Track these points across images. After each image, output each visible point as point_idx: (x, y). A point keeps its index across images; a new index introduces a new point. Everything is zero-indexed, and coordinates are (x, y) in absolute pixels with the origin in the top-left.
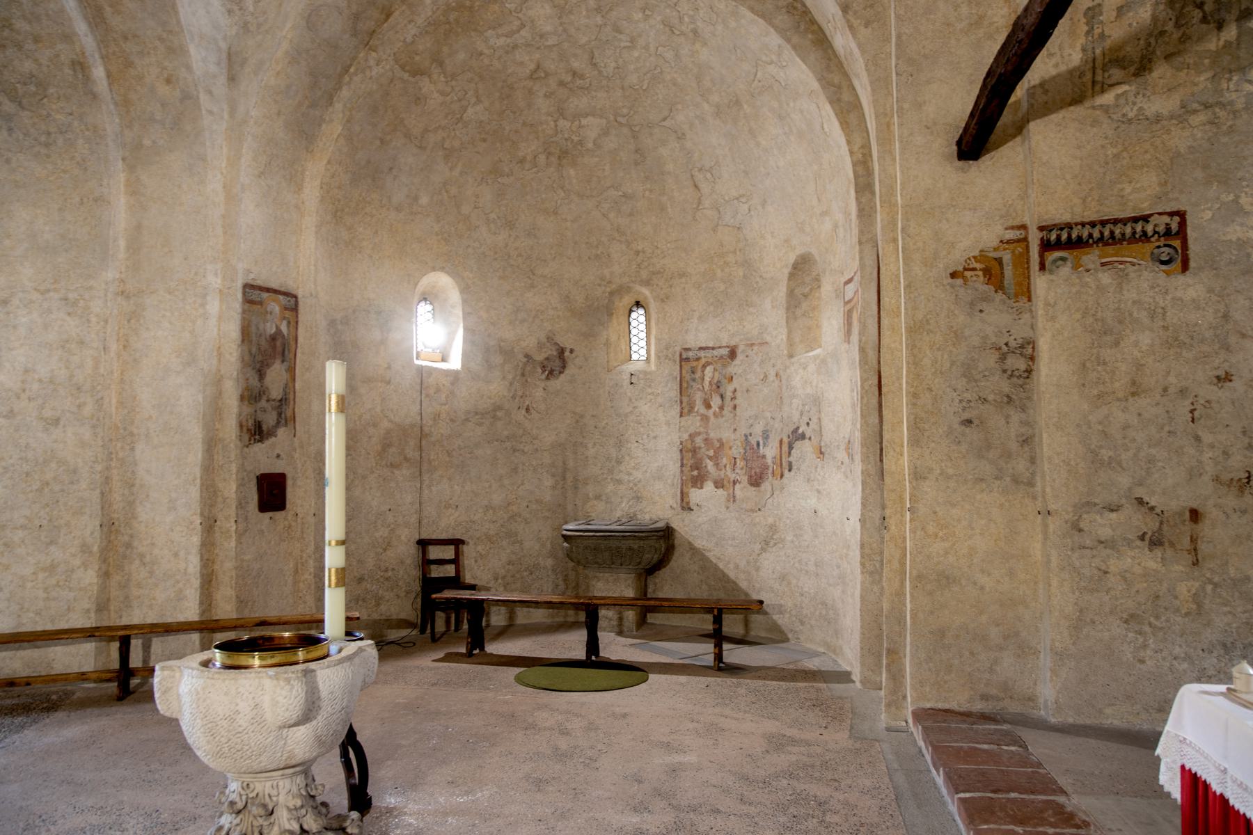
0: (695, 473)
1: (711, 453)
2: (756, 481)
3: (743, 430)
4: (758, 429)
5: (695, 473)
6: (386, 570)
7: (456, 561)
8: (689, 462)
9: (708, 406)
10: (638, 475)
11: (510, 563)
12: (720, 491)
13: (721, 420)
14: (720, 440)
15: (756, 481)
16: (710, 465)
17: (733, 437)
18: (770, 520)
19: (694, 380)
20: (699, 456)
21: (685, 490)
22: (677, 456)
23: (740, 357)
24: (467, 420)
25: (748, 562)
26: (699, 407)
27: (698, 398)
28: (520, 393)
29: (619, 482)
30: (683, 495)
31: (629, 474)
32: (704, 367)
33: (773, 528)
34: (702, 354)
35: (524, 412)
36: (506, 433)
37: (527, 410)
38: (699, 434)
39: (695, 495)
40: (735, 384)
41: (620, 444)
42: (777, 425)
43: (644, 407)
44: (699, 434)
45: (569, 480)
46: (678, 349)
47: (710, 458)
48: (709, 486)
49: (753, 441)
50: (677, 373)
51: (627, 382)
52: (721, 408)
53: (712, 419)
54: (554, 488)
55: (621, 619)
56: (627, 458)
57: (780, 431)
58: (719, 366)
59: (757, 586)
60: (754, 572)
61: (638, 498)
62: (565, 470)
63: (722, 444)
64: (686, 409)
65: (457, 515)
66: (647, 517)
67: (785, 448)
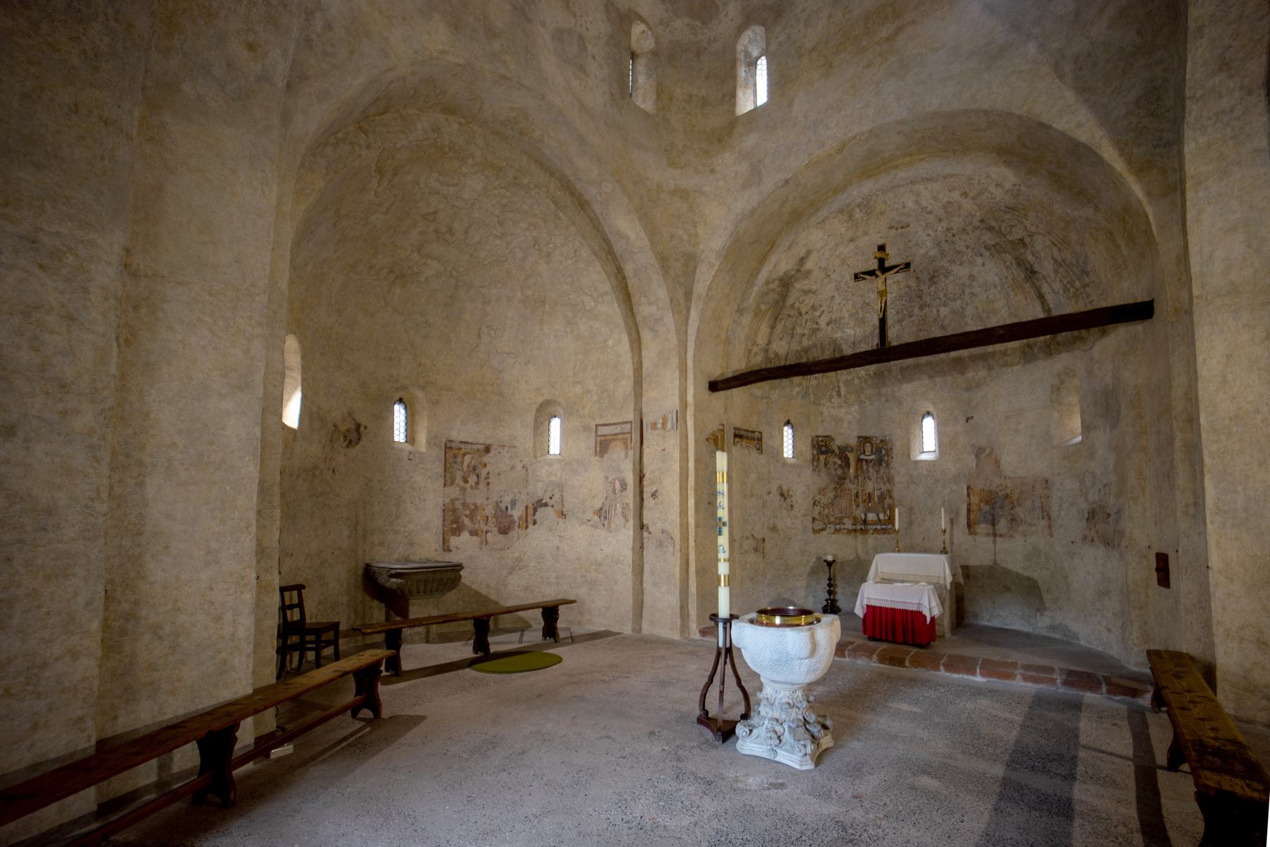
2: (504, 531)
3: (495, 498)
4: (507, 499)
9: (466, 481)
15: (504, 531)
16: (466, 521)
23: (493, 452)
26: (459, 481)
27: (459, 475)
32: (464, 455)
34: (463, 446)
46: (444, 440)
49: (503, 506)
50: (442, 456)
52: (477, 483)
57: (524, 500)
63: (476, 507)
67: (530, 511)
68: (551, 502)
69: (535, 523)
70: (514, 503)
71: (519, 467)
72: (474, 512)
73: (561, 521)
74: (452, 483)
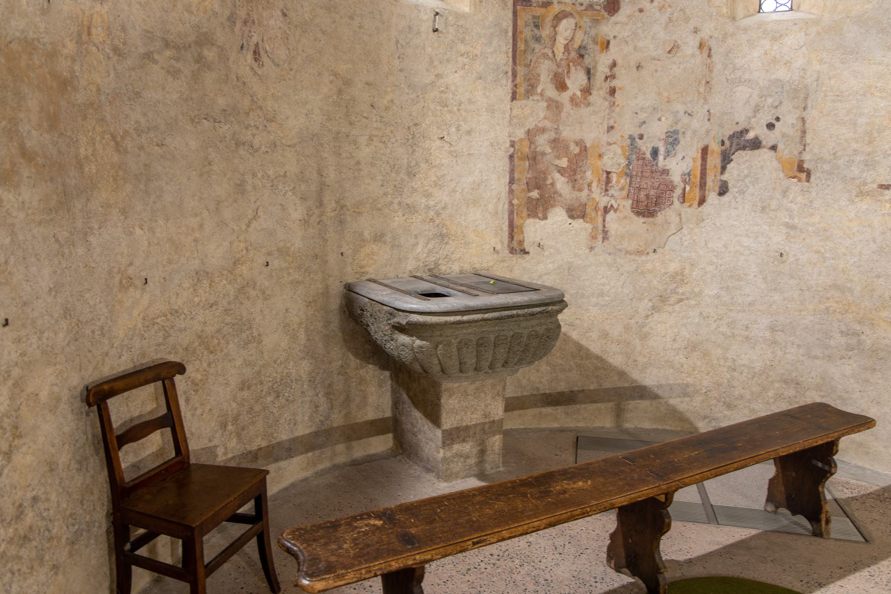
0: (535, 194)
1: (564, 163)
2: (646, 209)
3: (628, 128)
4: (656, 132)
5: (535, 194)
6: (20, 515)
7: (170, 420)
8: (524, 174)
9: (562, 87)
10: (441, 196)
11: (244, 385)
12: (579, 223)
13: (584, 111)
14: (580, 143)
15: (646, 209)
16: (561, 183)
17: (605, 138)
18: (673, 267)
19: (538, 39)
20: (542, 167)
21: (517, 221)
22: (503, 165)
24: (148, 56)
25: (627, 328)
26: (546, 85)
27: (545, 70)
28: (242, 13)
29: (411, 209)
30: (513, 229)
31: (428, 195)
32: (558, 18)
33: (679, 278)
35: (250, 57)
36: (221, 102)
37: (256, 53)
38: (543, 130)
39: (534, 230)
40: (614, 53)
41: (413, 140)
42: (697, 124)
43: (453, 78)
44: (543, 130)
45: (330, 208)
47: (561, 171)
48: (558, 215)
49: (646, 147)
50: (508, 24)
51: (426, 27)
52: (587, 91)
53: (568, 106)
54: (305, 222)
55: (482, 452)
56: (424, 166)
58: (586, 21)
59: (641, 360)
60: (637, 342)
61: (442, 236)
62: (322, 187)
63: (584, 149)
64: (522, 87)
65: (145, 301)
66: (456, 268)
67: (714, 160)
68: (769, 137)
69: (723, 190)
70: (673, 139)
71: (690, 46)
72: (578, 159)
73: (795, 186)
74: (531, 90)
